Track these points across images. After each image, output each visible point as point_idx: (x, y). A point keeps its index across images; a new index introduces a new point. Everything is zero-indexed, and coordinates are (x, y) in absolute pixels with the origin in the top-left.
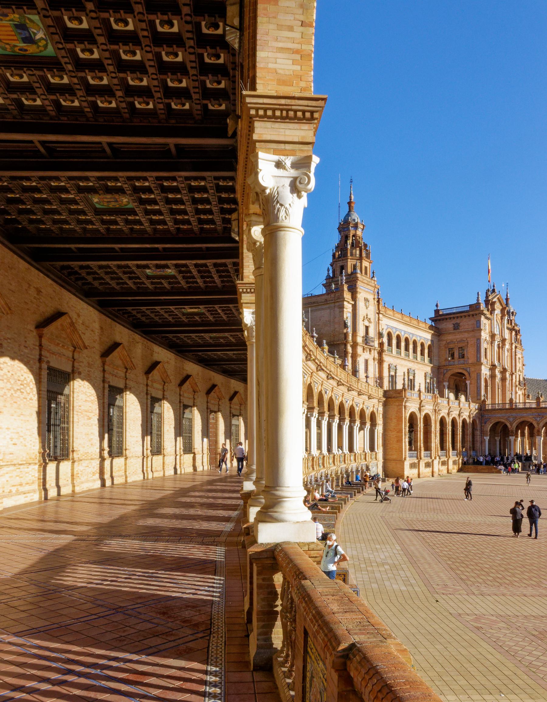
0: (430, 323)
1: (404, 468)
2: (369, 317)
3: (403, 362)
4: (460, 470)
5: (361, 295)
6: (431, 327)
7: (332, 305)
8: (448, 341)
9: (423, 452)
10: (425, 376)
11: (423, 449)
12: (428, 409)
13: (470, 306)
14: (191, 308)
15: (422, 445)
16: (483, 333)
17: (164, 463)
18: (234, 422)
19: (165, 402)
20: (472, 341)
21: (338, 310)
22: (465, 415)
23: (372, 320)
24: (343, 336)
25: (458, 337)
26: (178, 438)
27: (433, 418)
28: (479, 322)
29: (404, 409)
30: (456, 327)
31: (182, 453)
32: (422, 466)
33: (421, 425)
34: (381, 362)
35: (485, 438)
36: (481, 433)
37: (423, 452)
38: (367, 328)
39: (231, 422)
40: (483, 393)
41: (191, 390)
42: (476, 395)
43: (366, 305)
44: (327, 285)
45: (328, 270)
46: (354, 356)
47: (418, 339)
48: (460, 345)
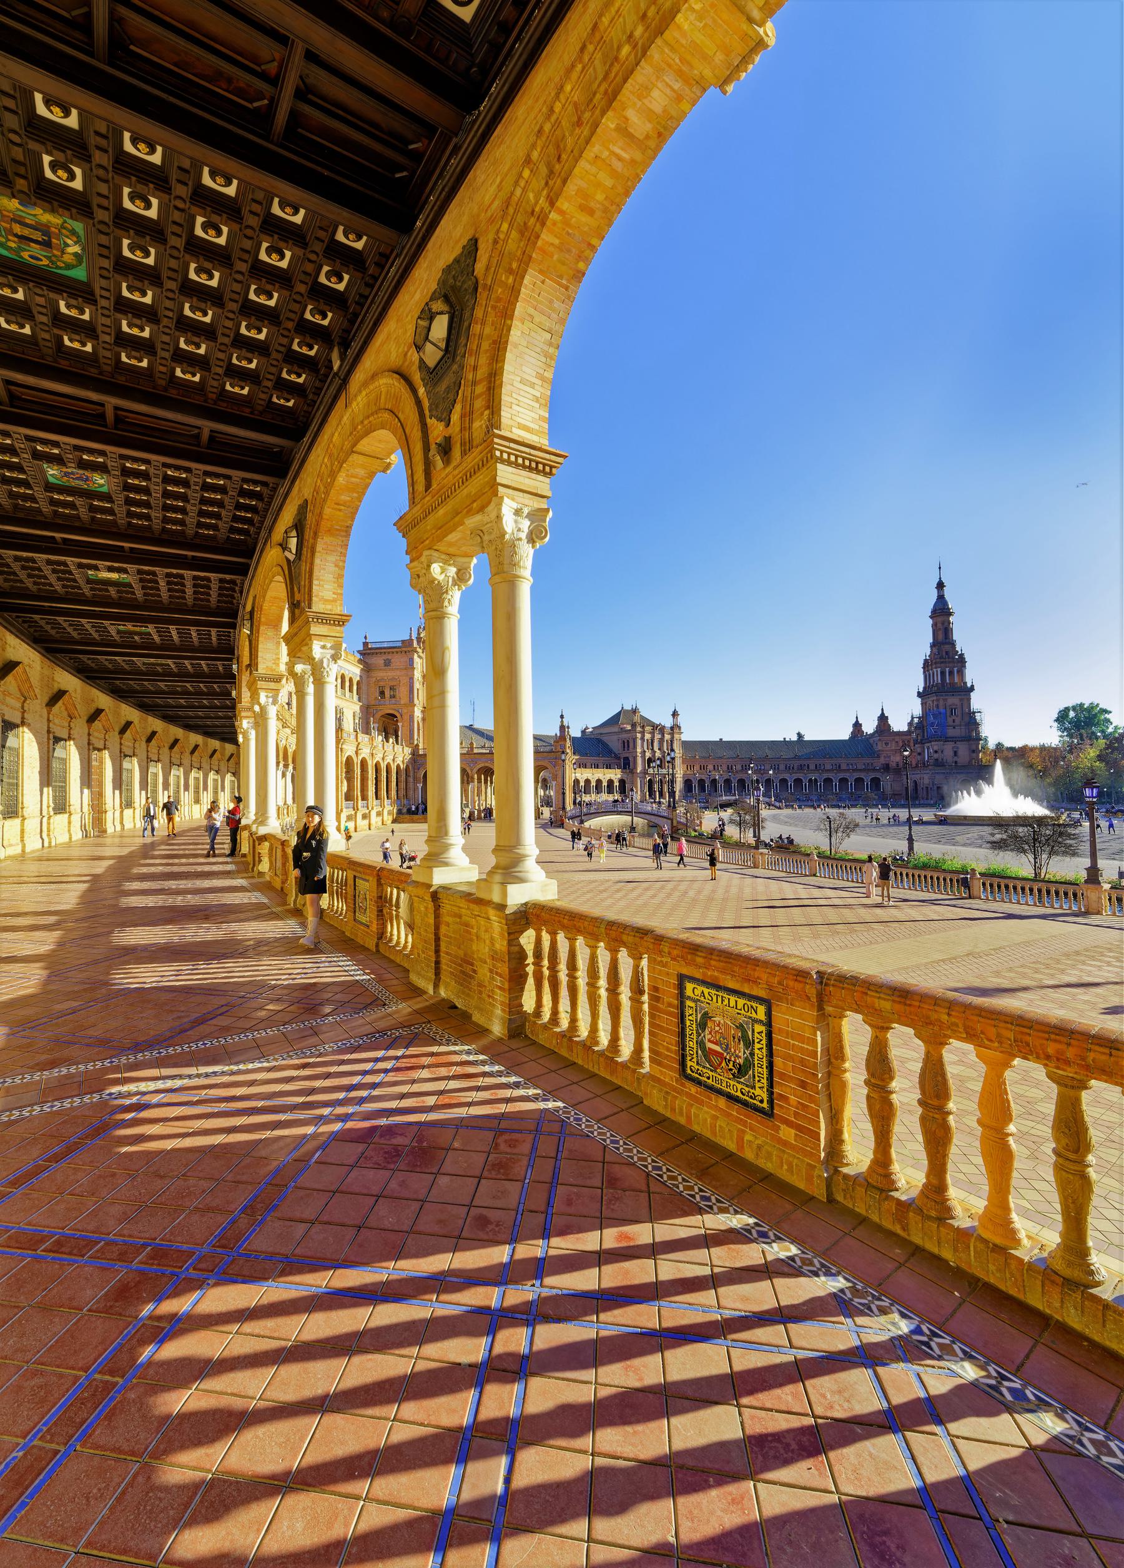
0: (358, 656)
4: (394, 821)
6: (360, 661)
9: (360, 802)
12: (365, 753)
13: (403, 641)
14: (111, 569)
16: (415, 672)
17: (22, 831)
18: (126, 764)
19: (26, 729)
22: (399, 761)
25: (390, 674)
26: (45, 790)
27: (370, 763)
28: (412, 660)
30: (387, 663)
31: (52, 813)
33: (358, 771)
37: (360, 802)
39: (121, 765)
40: (416, 737)
41: (65, 714)
47: (346, 673)
48: (392, 684)
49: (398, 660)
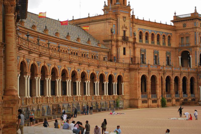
1: (138, 103)
2: (125, 26)
3: (150, 47)
7: (105, 21)
8: (180, 34)
10: (166, 54)
20: (192, 34)
23: (128, 27)
24: (110, 37)
25: (185, 31)
29: (138, 74)
30: (184, 26)
32: (150, 102)
33: (149, 81)
34: (134, 48)
35: (200, 87)
36: (197, 84)
38: (125, 31)
42: (195, 63)
43: (124, 20)
44: (104, 10)
45: (105, 2)
46: (117, 46)
49: (190, 24)
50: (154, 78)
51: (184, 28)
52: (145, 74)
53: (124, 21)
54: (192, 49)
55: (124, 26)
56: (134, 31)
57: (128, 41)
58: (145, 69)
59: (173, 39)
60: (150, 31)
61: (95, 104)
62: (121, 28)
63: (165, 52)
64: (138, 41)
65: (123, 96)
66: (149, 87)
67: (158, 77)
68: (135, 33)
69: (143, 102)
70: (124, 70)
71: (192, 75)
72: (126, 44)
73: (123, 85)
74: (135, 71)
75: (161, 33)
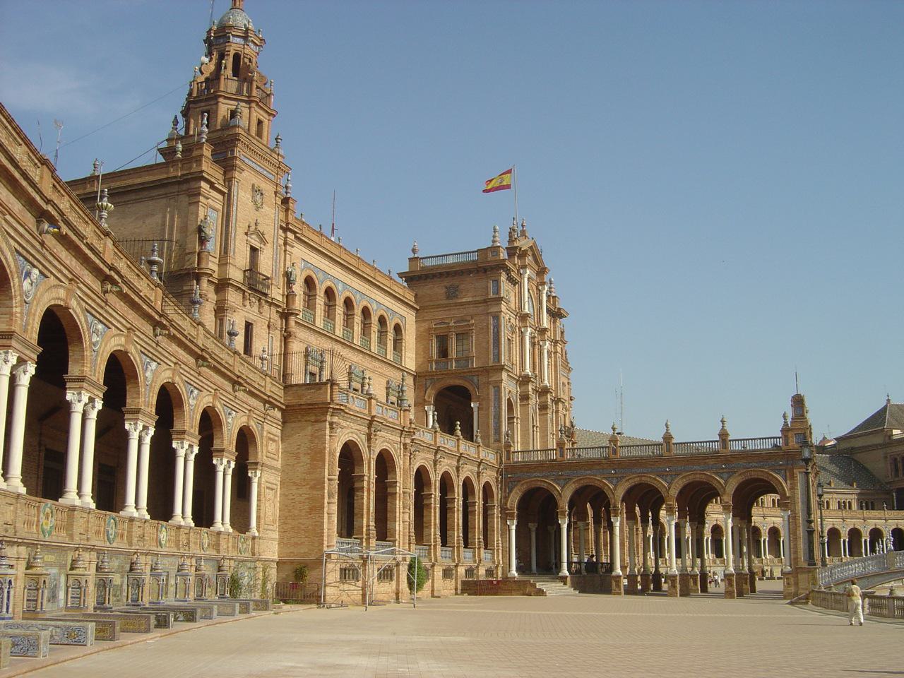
5: (245, 179)
7: (175, 189)
11: (373, 532)
15: (372, 523)
21: (187, 199)
27: (400, 462)
29: (328, 431)
30: (452, 293)
33: (369, 473)
40: (504, 427)
43: (255, 202)
45: (176, 122)
47: (373, 307)
50: (385, 463)
51: (451, 301)
52: (354, 437)
53: (254, 207)
54: (483, 379)
55: (253, 228)
56: (288, 264)
57: (266, 295)
58: (356, 417)
59: (407, 337)
60: (340, 287)
61: (120, 570)
62: (241, 231)
63: (384, 382)
64: (299, 303)
65: (254, 538)
66: (367, 500)
67: (401, 462)
68: (294, 273)
69: (347, 574)
70: (269, 402)
71: (489, 476)
72: (255, 308)
73: (255, 480)
74: (313, 418)
75: (375, 306)
